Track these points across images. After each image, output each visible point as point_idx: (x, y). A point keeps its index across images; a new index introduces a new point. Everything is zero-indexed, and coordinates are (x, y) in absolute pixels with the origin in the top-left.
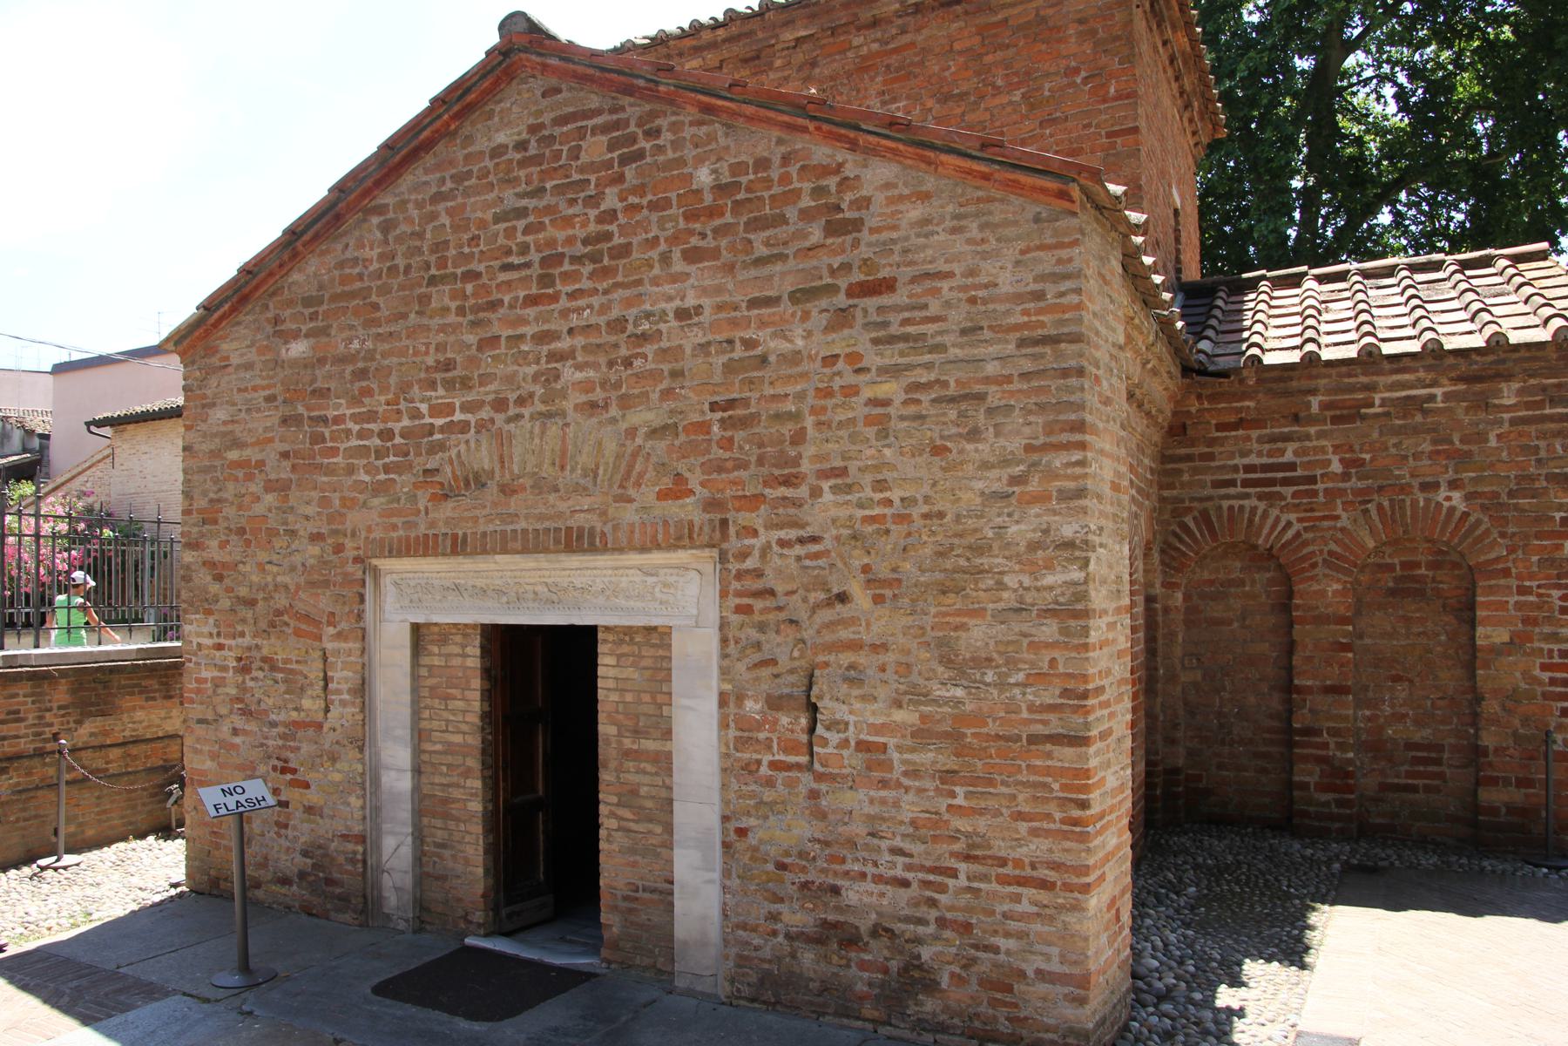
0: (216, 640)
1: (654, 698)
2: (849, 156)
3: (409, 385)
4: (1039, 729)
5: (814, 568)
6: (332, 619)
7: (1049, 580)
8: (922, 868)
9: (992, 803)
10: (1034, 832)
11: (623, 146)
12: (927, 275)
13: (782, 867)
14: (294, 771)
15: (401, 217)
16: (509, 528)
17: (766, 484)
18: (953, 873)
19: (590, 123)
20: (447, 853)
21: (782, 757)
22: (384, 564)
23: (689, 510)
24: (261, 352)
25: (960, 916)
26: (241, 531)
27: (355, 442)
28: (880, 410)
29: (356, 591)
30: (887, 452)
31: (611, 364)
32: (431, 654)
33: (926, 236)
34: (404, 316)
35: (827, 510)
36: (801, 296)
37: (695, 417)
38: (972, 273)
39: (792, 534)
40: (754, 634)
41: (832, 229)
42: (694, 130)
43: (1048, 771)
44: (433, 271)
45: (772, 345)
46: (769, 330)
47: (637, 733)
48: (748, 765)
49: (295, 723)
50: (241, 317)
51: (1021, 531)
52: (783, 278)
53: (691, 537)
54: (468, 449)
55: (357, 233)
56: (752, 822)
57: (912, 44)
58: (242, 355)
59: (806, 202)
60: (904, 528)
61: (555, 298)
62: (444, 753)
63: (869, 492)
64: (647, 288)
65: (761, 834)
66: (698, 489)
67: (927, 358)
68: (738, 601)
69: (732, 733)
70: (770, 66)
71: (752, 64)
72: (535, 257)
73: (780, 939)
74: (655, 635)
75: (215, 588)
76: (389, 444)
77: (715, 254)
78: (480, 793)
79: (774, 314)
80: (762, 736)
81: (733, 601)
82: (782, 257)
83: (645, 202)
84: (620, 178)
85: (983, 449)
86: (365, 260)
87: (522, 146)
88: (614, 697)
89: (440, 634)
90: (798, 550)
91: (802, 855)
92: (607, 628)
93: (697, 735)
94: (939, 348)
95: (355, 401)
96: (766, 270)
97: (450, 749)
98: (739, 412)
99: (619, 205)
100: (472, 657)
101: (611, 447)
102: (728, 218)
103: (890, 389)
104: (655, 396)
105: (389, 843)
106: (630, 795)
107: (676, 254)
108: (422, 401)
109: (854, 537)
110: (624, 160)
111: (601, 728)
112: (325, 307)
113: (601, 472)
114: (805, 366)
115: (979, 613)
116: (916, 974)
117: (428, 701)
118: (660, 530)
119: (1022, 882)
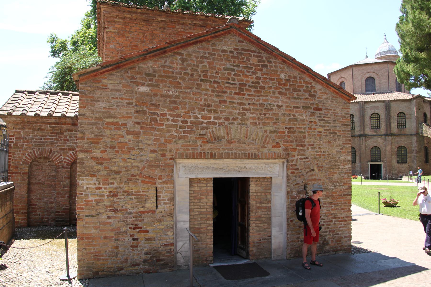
0: (97, 186)
4: (345, 193)
6: (160, 177)
7: (346, 167)
9: (338, 207)
10: (344, 212)
11: (262, 62)
12: (327, 109)
14: (141, 228)
15: (189, 59)
16: (230, 152)
17: (297, 146)
18: (332, 221)
19: (253, 54)
20: (199, 243)
22: (178, 160)
23: (280, 150)
24: (124, 86)
25: (332, 229)
26: (113, 147)
27: (170, 122)
28: (319, 133)
29: (170, 169)
30: (321, 142)
31: (261, 114)
32: (194, 187)
34: (191, 88)
35: (310, 152)
36: (305, 108)
37: (282, 130)
38: (334, 110)
39: (303, 157)
40: (294, 178)
41: (311, 95)
42: (280, 65)
43: (346, 200)
44: (202, 78)
45: (299, 117)
47: (261, 202)
49: (141, 212)
50: (114, 73)
51: (342, 158)
52: (301, 103)
53: (280, 157)
54: (216, 130)
55: (171, 59)
58: (114, 86)
59: (305, 88)
60: (324, 156)
61: (244, 95)
64: (269, 98)
66: (282, 146)
67: (328, 125)
69: (290, 200)
70: (152, 25)
72: (238, 83)
73: (300, 242)
75: (97, 167)
76: (186, 125)
77: (285, 94)
81: (290, 171)
83: (268, 77)
84: (261, 70)
85: (336, 143)
86: (173, 68)
87: (231, 52)
88: (255, 194)
89: (198, 181)
90: (304, 160)
92: (253, 178)
94: (330, 123)
95: (170, 110)
96: (297, 101)
97: (201, 213)
98: (292, 130)
99: (261, 76)
100: (210, 186)
101: (260, 134)
102: (288, 87)
103: (321, 130)
104: (271, 124)
105: (180, 244)
106: (259, 218)
107: (277, 92)
108: (199, 114)
109: (315, 158)
110: (263, 66)
111: (251, 202)
112: (156, 78)
113: (257, 140)
114: (305, 123)
115: (336, 173)
116: (325, 242)
117: (193, 200)
118: (273, 155)
119: (342, 221)
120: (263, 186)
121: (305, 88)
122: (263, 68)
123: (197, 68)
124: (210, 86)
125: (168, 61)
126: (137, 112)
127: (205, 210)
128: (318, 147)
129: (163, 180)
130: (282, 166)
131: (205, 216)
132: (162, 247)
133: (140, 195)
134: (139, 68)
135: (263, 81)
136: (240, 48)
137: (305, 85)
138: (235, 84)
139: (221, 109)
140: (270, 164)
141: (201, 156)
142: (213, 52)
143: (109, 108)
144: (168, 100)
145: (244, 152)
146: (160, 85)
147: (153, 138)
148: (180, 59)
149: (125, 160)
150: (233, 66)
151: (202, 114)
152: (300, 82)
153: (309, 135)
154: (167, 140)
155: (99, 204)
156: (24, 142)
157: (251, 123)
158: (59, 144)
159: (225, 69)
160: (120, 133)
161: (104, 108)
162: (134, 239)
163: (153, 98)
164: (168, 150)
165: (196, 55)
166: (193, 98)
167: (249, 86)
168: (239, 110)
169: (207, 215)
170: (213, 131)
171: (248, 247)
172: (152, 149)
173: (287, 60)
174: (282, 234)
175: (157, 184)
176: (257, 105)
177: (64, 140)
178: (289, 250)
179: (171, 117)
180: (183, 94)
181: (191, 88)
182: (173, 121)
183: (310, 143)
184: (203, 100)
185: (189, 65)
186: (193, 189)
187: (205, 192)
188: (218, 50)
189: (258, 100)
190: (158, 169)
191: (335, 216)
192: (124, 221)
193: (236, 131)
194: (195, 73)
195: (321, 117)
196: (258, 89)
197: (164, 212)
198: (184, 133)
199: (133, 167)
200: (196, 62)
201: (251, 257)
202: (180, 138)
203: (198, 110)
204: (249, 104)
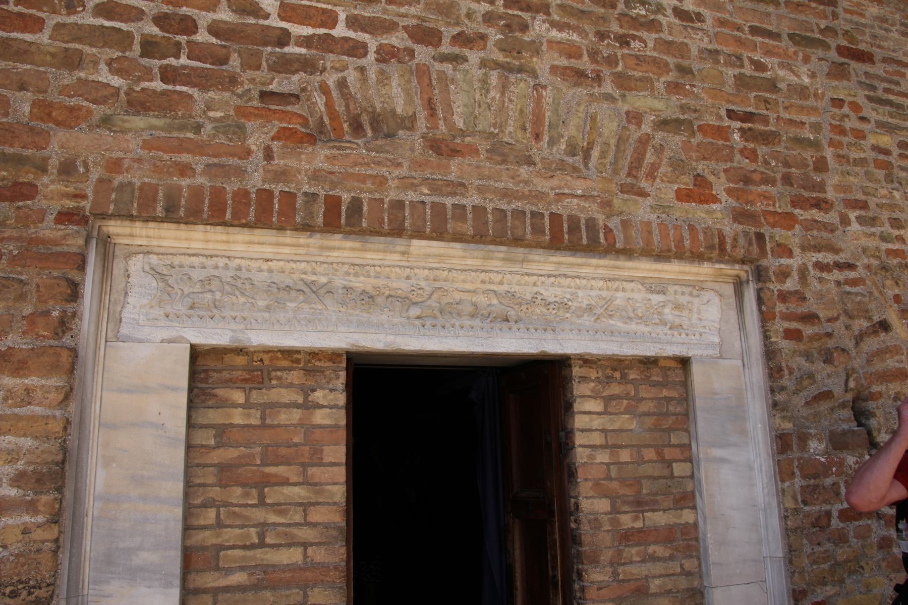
1: (660, 454)
5: (857, 294)
16: (449, 201)
17: (794, 204)
23: (715, 216)
28: (881, 157)
30: (896, 194)
31: (602, 36)
32: (224, 404)
33: (886, 30)
45: (781, 73)
47: (640, 505)
48: (818, 519)
66: (723, 196)
68: (786, 325)
69: (798, 482)
74: (655, 370)
76: (183, 39)
79: (777, 46)
80: (828, 481)
81: (780, 326)
88: (603, 457)
89: (248, 369)
90: (837, 275)
92: (587, 361)
100: (331, 405)
101: (609, 128)
103: (885, 140)
104: (660, 86)
111: (586, 505)
113: (595, 153)
114: (811, 102)
117: (215, 492)
118: (686, 235)
120: (644, 407)
127: (292, 556)
130: (732, 300)
140: (671, 289)
141: (265, 211)
145: (528, 208)
157: (554, 69)
164: (54, 163)
169: (305, 587)
170: (342, 84)
186: (213, 416)
195: (873, 88)
202: (139, 104)
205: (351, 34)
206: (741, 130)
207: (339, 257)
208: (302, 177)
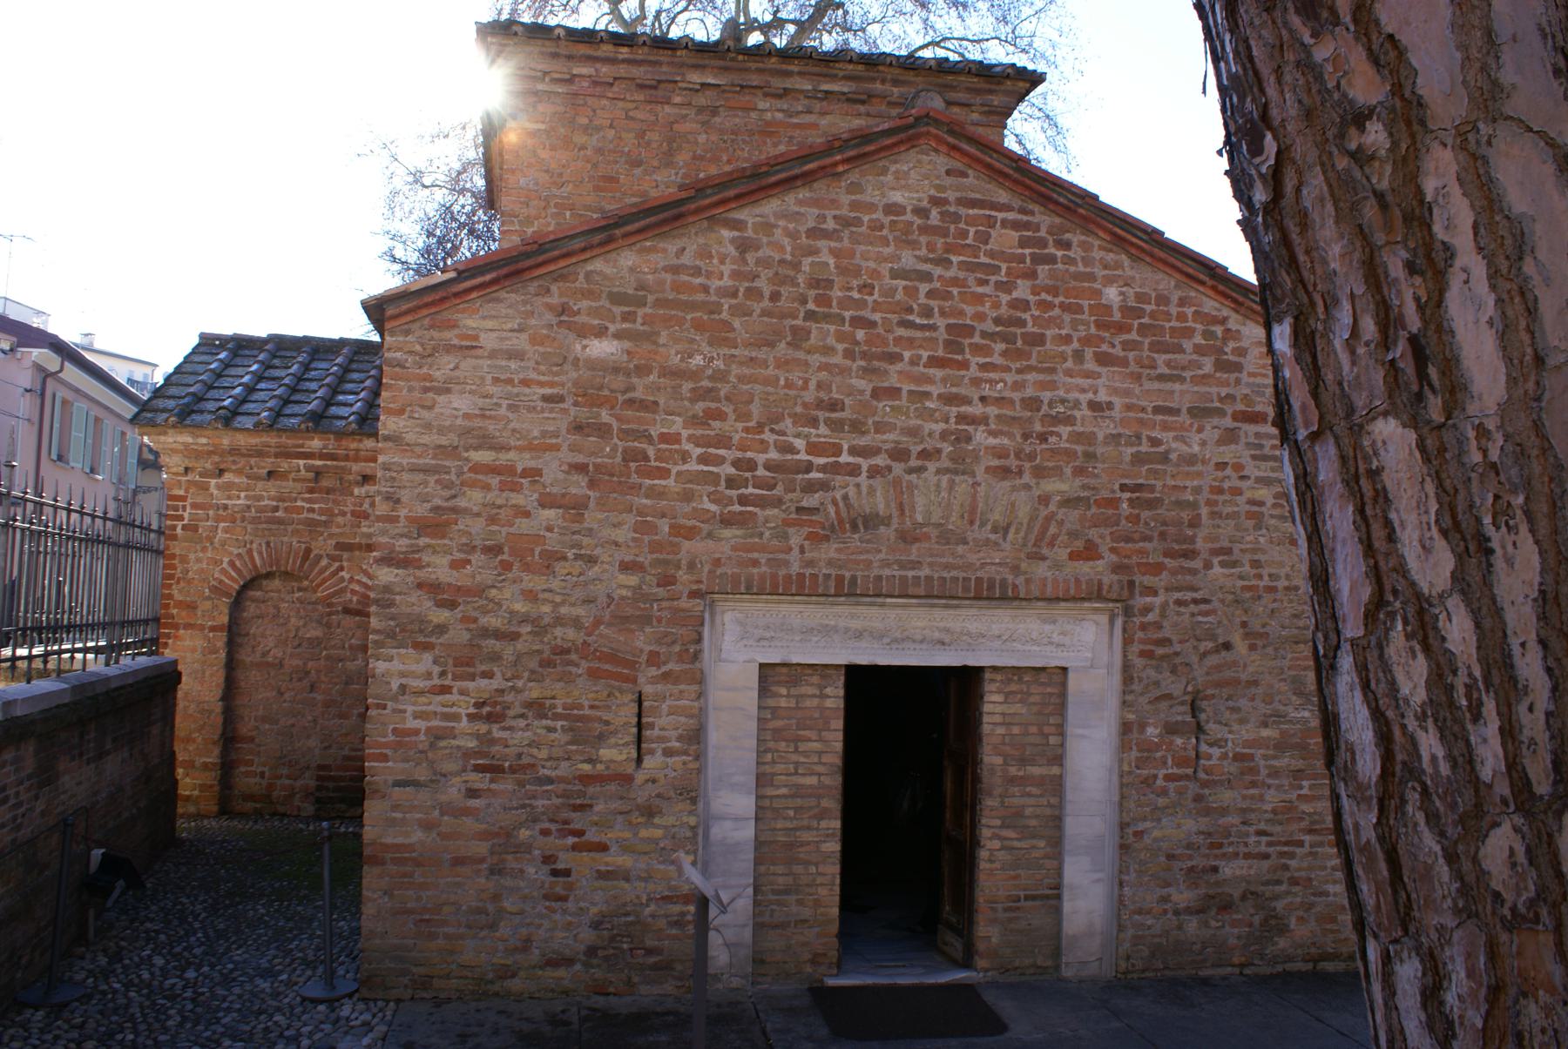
0: (436, 681)
2: (1234, 315)
3: (779, 418)
6: (654, 659)
8: (1279, 843)
13: (1170, 857)
14: (580, 833)
15: (765, 240)
16: (910, 574)
17: (1166, 555)
18: (1301, 844)
19: (1000, 215)
20: (792, 898)
21: (1175, 770)
23: (1097, 570)
24: (534, 341)
27: (693, 466)
30: (1262, 540)
32: (776, 695)
34: (772, 345)
36: (1200, 413)
37: (1105, 494)
39: (1189, 595)
40: (1152, 673)
41: (1222, 366)
42: (1102, 253)
44: (811, 306)
46: (1172, 434)
47: (1023, 761)
48: (1147, 779)
49: (586, 779)
50: (502, 294)
54: (859, 493)
55: (701, 240)
56: (1148, 824)
57: (815, 126)
59: (1198, 339)
60: (1271, 596)
61: (964, 365)
62: (793, 796)
63: (1247, 568)
64: (1060, 377)
65: (1156, 833)
66: (1106, 554)
69: (1134, 754)
71: (648, 92)
72: (941, 323)
75: (441, 616)
76: (748, 474)
77: (1124, 362)
78: (839, 833)
82: (1182, 380)
83: (1057, 301)
84: (1032, 275)
87: (921, 212)
88: (1001, 730)
91: (1189, 846)
92: (995, 669)
93: (1091, 757)
96: (1168, 386)
97: (798, 792)
99: (1031, 298)
100: (835, 696)
101: (1023, 512)
102: (1134, 336)
103: (1264, 493)
104: (1068, 471)
106: (1013, 818)
107: (1089, 353)
108: (798, 436)
110: (1036, 259)
111: (986, 759)
112: (648, 310)
113: (1012, 530)
114: (1199, 467)
117: (771, 744)
118: (1072, 586)
120: (1032, 699)
121: (1198, 339)
122: (1040, 268)
123: (792, 273)
124: (841, 337)
125: (692, 248)
126: (578, 428)
127: (812, 781)
128: (1248, 556)
129: (664, 669)
130: (1107, 627)
131: (813, 802)
132: (653, 907)
133: (580, 718)
134: (588, 275)
135: (1037, 313)
136: (951, 195)
137: (1198, 326)
138: (933, 328)
139: (876, 419)
141: (801, 588)
142: (853, 215)
143: (483, 416)
144: (687, 386)
145: (962, 575)
146: (658, 334)
147: (631, 519)
148: (733, 241)
149: (531, 596)
150: (927, 260)
151: (807, 436)
152: (1182, 317)
153: (1213, 515)
154: (681, 527)
155: (442, 744)
156: (218, 519)
157: (988, 469)
158: (335, 530)
159: (895, 275)
160: (517, 499)
161: (466, 416)
162: (555, 873)
163: (635, 380)
165: (791, 226)
166: (778, 379)
167: (984, 334)
168: (947, 422)
169: (819, 797)
170: (845, 497)
171: (971, 922)
172: (628, 558)
173: (1129, 237)
174: (1098, 881)
175: (641, 680)
176: (1012, 402)
177: (353, 513)
178: (1127, 945)
179: (698, 445)
180: (741, 364)
181: (772, 345)
182: (703, 460)
183: (1217, 545)
184: (812, 385)
185: (765, 263)
186: (771, 702)
187: (817, 715)
188: (871, 207)
189: (1017, 386)
190: (648, 630)
191: (1312, 823)
192: (524, 806)
193: (930, 496)
194: (785, 291)
195: (1261, 446)
196: (1019, 343)
197: (663, 781)
198: (740, 504)
199: (559, 621)
200: (789, 249)
201: (981, 963)
202: (727, 521)
203: (794, 423)
204: (983, 399)
205: (851, 459)
206: (1130, 500)
207: (841, 614)
208: (822, 564)
